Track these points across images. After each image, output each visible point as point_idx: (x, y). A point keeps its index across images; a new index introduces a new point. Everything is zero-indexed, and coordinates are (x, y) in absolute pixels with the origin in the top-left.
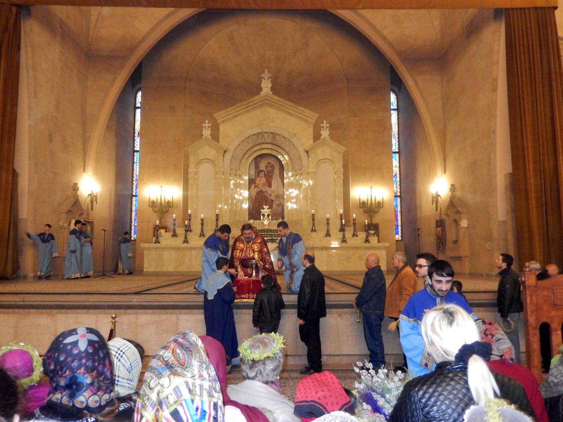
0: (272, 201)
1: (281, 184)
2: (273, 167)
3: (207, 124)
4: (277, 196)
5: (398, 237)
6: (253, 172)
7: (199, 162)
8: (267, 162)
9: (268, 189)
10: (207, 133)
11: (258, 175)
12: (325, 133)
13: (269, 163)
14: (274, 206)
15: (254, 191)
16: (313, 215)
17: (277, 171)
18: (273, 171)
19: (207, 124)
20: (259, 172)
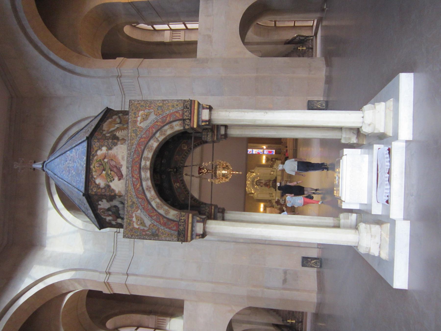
0: (266, 182)
3: (250, 195)
4: (265, 181)
5: (274, 151)
10: (252, 195)
12: (253, 171)
15: (264, 186)
17: (260, 181)
18: (260, 182)
19: (250, 195)
20: (260, 185)
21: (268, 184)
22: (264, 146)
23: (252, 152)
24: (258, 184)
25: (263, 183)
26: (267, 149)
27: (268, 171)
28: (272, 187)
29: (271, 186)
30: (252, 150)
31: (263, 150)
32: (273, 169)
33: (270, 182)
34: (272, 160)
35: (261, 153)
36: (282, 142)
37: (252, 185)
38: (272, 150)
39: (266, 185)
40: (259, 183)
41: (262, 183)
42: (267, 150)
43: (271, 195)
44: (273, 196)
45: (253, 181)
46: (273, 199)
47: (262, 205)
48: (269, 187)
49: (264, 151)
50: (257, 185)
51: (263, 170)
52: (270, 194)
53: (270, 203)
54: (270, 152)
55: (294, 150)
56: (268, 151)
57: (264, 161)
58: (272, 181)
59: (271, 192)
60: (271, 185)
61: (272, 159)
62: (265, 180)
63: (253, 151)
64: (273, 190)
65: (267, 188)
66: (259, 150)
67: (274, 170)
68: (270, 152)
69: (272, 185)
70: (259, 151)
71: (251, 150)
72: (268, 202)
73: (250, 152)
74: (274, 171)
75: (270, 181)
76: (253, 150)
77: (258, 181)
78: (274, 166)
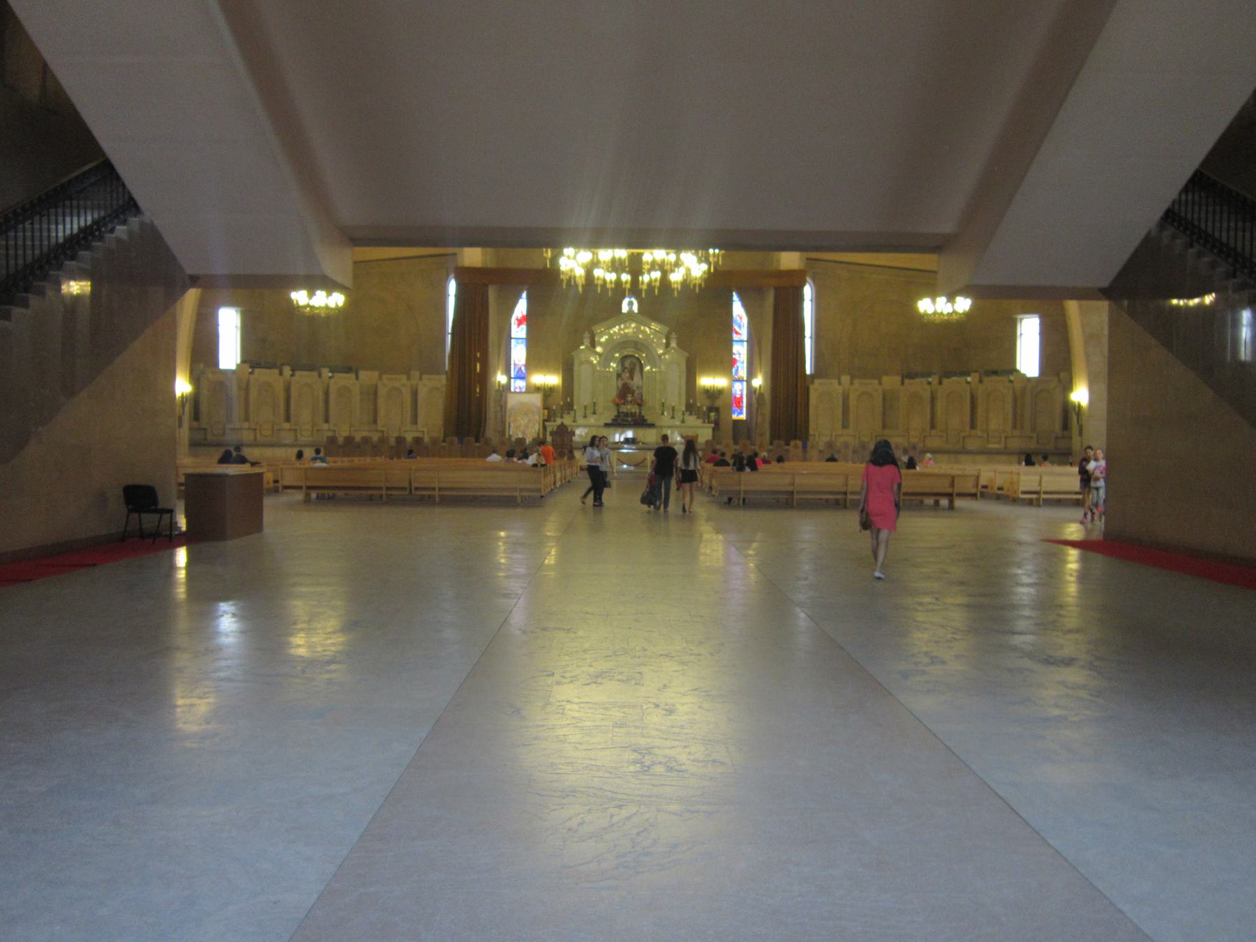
0: (634, 391)
1: (640, 377)
2: (635, 365)
3: (587, 335)
4: (638, 387)
5: (743, 417)
6: (620, 368)
7: (581, 363)
8: (629, 361)
9: (631, 382)
11: (624, 371)
12: (673, 344)
13: (631, 362)
14: (636, 394)
15: (620, 383)
16: (663, 403)
17: (638, 368)
19: (587, 335)
20: (624, 368)
21: (629, 399)
22: (765, 379)
23: (738, 339)
24: (627, 364)
25: (629, 381)
26: (750, 390)
27: (676, 398)
28: (618, 412)
29: (621, 411)
30: (746, 339)
31: (745, 379)
32: (683, 414)
33: (636, 406)
34: (710, 409)
35: (734, 370)
36: (788, 444)
37: (624, 343)
38: (745, 410)
39: (625, 392)
40: (631, 365)
41: (632, 378)
42: (745, 393)
43: (589, 411)
44: (585, 416)
45: (637, 344)
46: (575, 417)
47: (552, 380)
48: (617, 400)
49: (743, 381)
50: (624, 359)
51: (676, 377)
52: (594, 404)
53: (562, 406)
54: (739, 401)
55: (792, 492)
56: (742, 397)
57: (707, 381)
58: (637, 411)
59: (599, 409)
60: (624, 409)
61: (717, 410)
62: (642, 388)
63: (743, 346)
64: (609, 416)
65: (613, 393)
66: (745, 365)
67: (679, 415)
68: (739, 401)
69: (625, 411)
70: (743, 363)
71: (744, 336)
72: (566, 400)
73: (737, 333)
74: (676, 417)
75: (640, 405)
76: (745, 344)
77: (634, 360)
78: (693, 418)
